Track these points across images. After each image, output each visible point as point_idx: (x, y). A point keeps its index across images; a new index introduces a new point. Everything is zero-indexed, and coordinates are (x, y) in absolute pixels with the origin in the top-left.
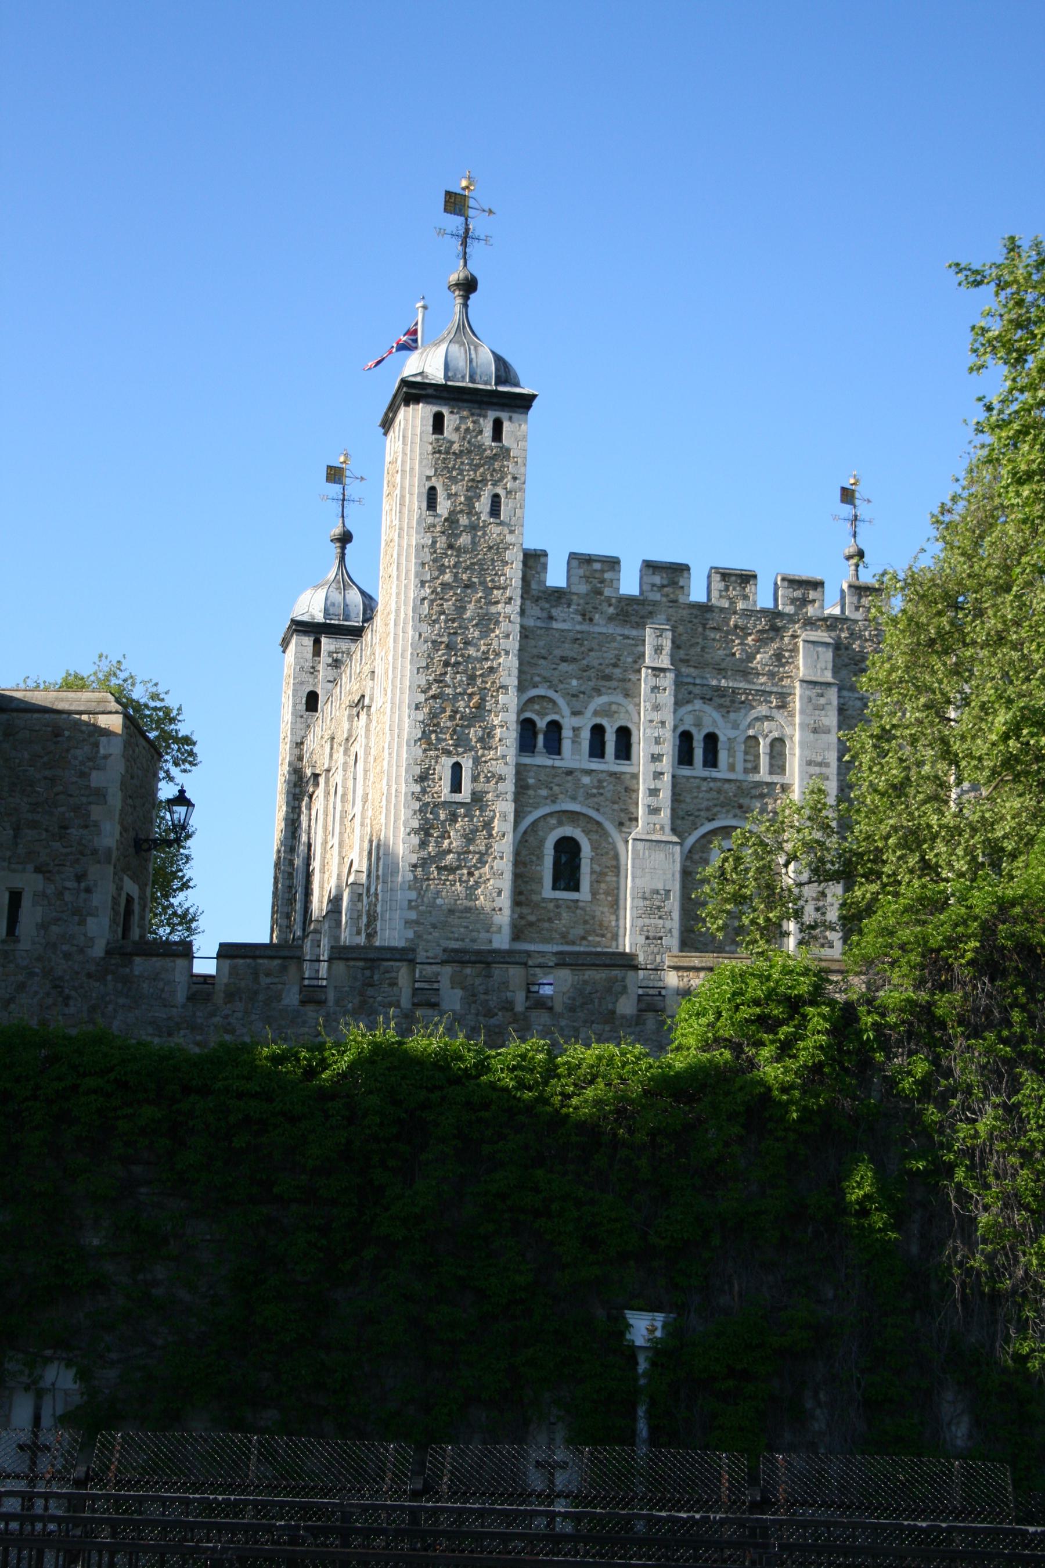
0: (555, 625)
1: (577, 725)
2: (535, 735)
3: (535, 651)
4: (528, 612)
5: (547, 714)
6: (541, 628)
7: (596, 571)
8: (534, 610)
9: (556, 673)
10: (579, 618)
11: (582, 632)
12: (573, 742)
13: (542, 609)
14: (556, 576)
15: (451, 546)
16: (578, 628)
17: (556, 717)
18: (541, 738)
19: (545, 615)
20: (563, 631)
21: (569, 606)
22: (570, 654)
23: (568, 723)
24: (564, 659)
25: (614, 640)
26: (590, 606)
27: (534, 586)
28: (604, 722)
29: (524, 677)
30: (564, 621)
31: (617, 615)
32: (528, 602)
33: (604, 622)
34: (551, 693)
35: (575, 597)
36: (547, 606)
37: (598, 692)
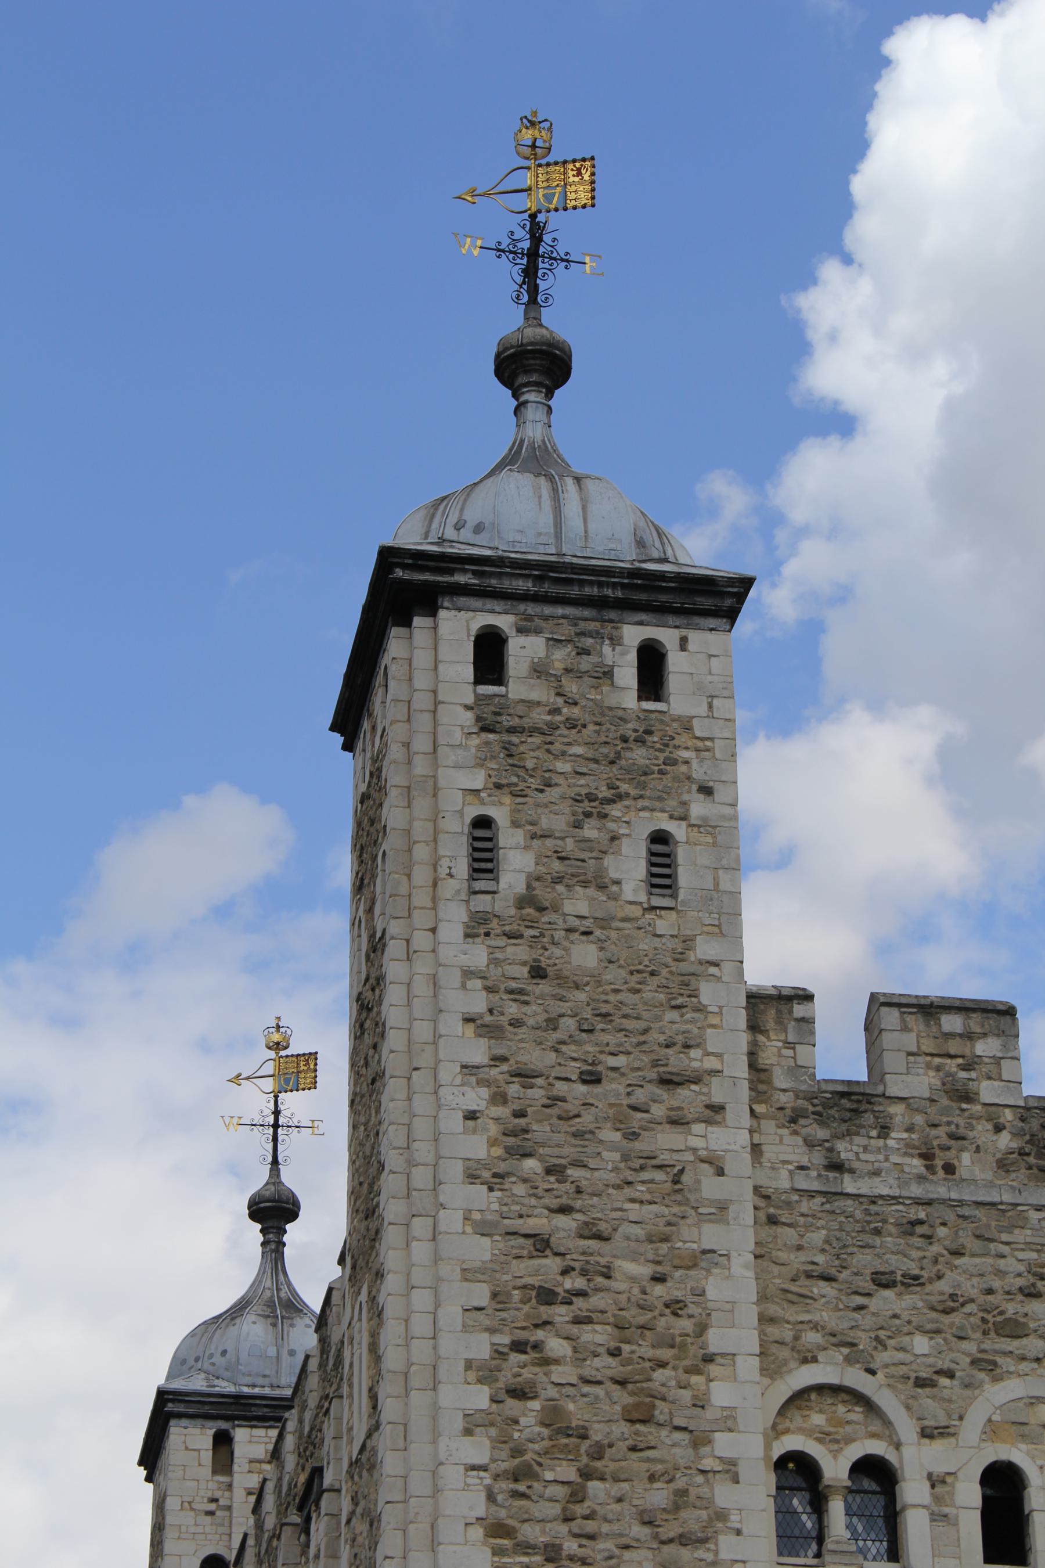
0: (849, 1185)
1: (939, 1469)
2: (818, 1504)
3: (797, 1261)
4: (770, 1152)
5: (849, 1440)
6: (811, 1194)
7: (950, 1035)
8: (786, 1148)
9: (866, 1320)
10: (917, 1165)
11: (929, 1203)
12: (938, 1517)
13: (810, 1144)
14: (838, 1054)
15: (538, 973)
16: (916, 1190)
17: (877, 1448)
18: (836, 1508)
19: (818, 1158)
20: (873, 1200)
21: (884, 1131)
22: (900, 1265)
23: (915, 1462)
24: (883, 1281)
25: (1022, 1223)
26: (941, 1131)
27: (780, 1080)
28: (1018, 1455)
29: (774, 1332)
30: (877, 1173)
31: (1022, 1153)
32: (769, 1126)
33: (989, 1175)
34: (855, 1378)
35: (897, 1110)
36: (822, 1134)
37: (987, 1366)
